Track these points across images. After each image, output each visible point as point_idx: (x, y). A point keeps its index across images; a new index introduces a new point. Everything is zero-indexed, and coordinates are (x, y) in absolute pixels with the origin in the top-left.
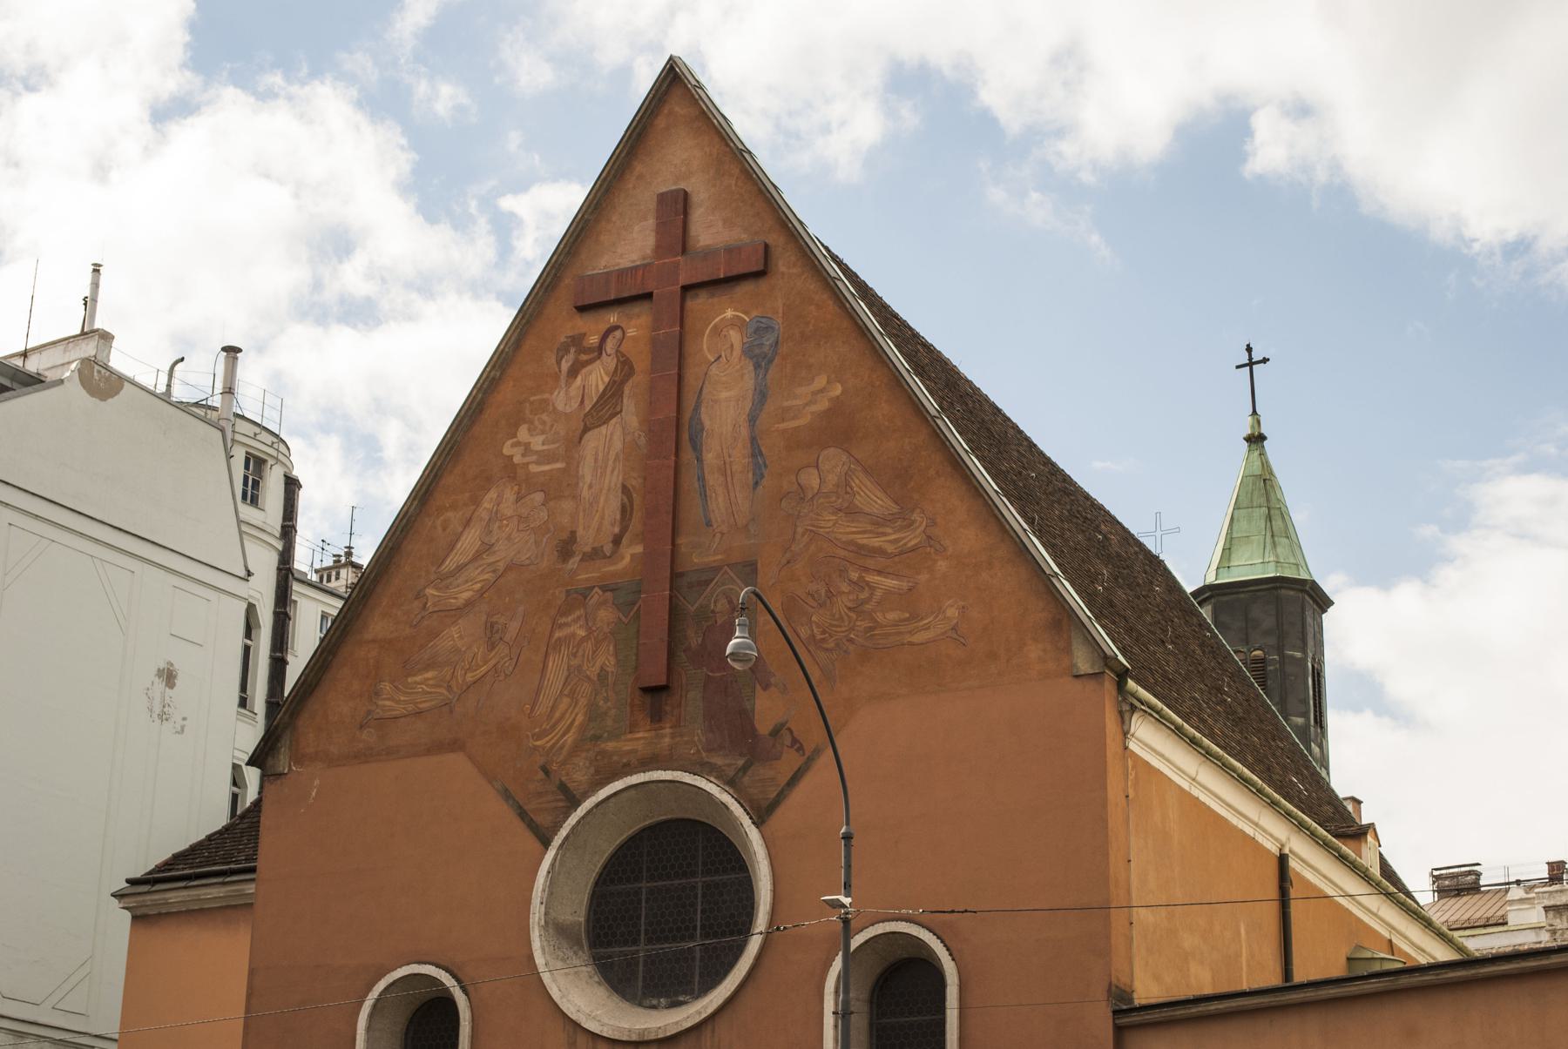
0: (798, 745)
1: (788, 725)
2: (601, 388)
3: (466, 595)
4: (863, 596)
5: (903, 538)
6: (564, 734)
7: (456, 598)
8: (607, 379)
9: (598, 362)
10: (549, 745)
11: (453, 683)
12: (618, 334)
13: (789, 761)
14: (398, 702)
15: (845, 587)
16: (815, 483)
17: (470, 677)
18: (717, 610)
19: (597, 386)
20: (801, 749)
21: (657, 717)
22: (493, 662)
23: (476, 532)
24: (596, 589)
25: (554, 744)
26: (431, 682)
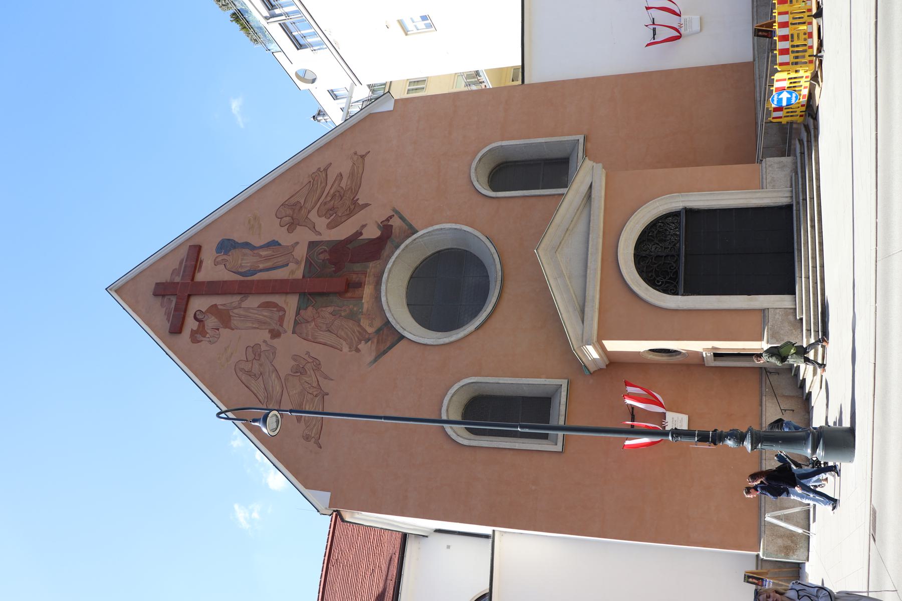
0: (389, 218)
1: (380, 223)
2: (216, 320)
3: (278, 388)
4: (338, 195)
5: (321, 181)
6: (354, 332)
7: (278, 393)
8: (213, 318)
9: (206, 323)
10: (356, 338)
11: (315, 393)
12: (197, 313)
13: (396, 222)
14: (315, 425)
15: (332, 203)
16: (288, 219)
17: (315, 384)
18: (323, 258)
19: (214, 322)
20: (391, 217)
21: (360, 285)
22: (312, 371)
23: (253, 383)
24: (297, 318)
25: (358, 338)
26: (311, 406)
